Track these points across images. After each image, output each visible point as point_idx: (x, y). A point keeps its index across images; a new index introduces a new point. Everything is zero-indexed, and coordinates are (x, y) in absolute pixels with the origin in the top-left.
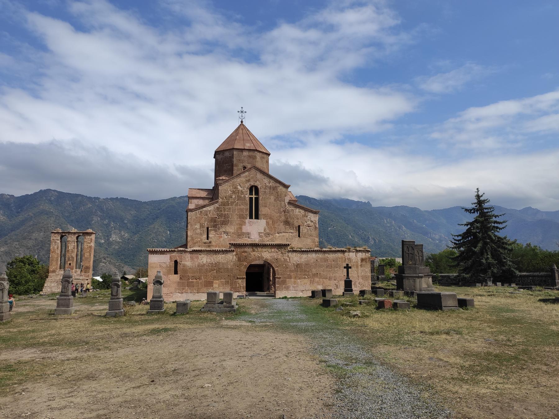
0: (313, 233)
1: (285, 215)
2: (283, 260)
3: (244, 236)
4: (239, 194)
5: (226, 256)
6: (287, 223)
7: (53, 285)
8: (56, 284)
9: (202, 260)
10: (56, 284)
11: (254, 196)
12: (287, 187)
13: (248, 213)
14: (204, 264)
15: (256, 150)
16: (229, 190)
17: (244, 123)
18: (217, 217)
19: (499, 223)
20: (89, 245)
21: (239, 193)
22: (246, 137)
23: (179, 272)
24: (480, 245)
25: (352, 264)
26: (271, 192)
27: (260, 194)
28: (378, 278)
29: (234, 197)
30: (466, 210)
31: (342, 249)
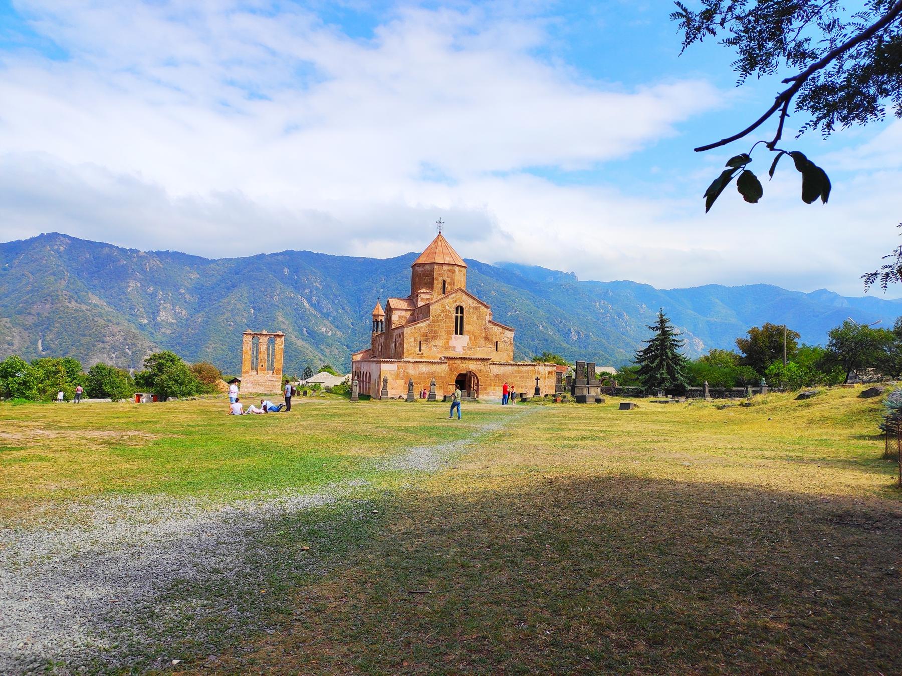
0: (508, 347)
6: (487, 338)
7: (248, 385)
8: (251, 385)
10: (251, 385)
11: (459, 315)
13: (454, 329)
15: (456, 265)
19: (677, 341)
20: (280, 347)
22: (445, 251)
24: (657, 361)
28: (565, 388)
29: (442, 315)
30: (650, 327)
31: (533, 363)
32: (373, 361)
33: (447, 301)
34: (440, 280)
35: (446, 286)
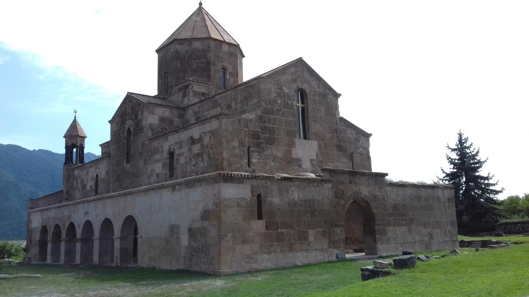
1: (337, 136)
2: (381, 197)
3: (295, 163)
4: (285, 99)
5: (321, 189)
6: (340, 148)
9: (292, 194)
11: (300, 105)
12: (337, 96)
13: (297, 129)
14: (296, 202)
16: (273, 90)
17: (203, 6)
18: (261, 132)
21: (285, 96)
23: (264, 215)
25: (441, 205)
26: (321, 101)
27: (309, 102)
29: (279, 102)
32: (164, 187)
33: (283, 78)
34: (219, 67)
35: (228, 77)
